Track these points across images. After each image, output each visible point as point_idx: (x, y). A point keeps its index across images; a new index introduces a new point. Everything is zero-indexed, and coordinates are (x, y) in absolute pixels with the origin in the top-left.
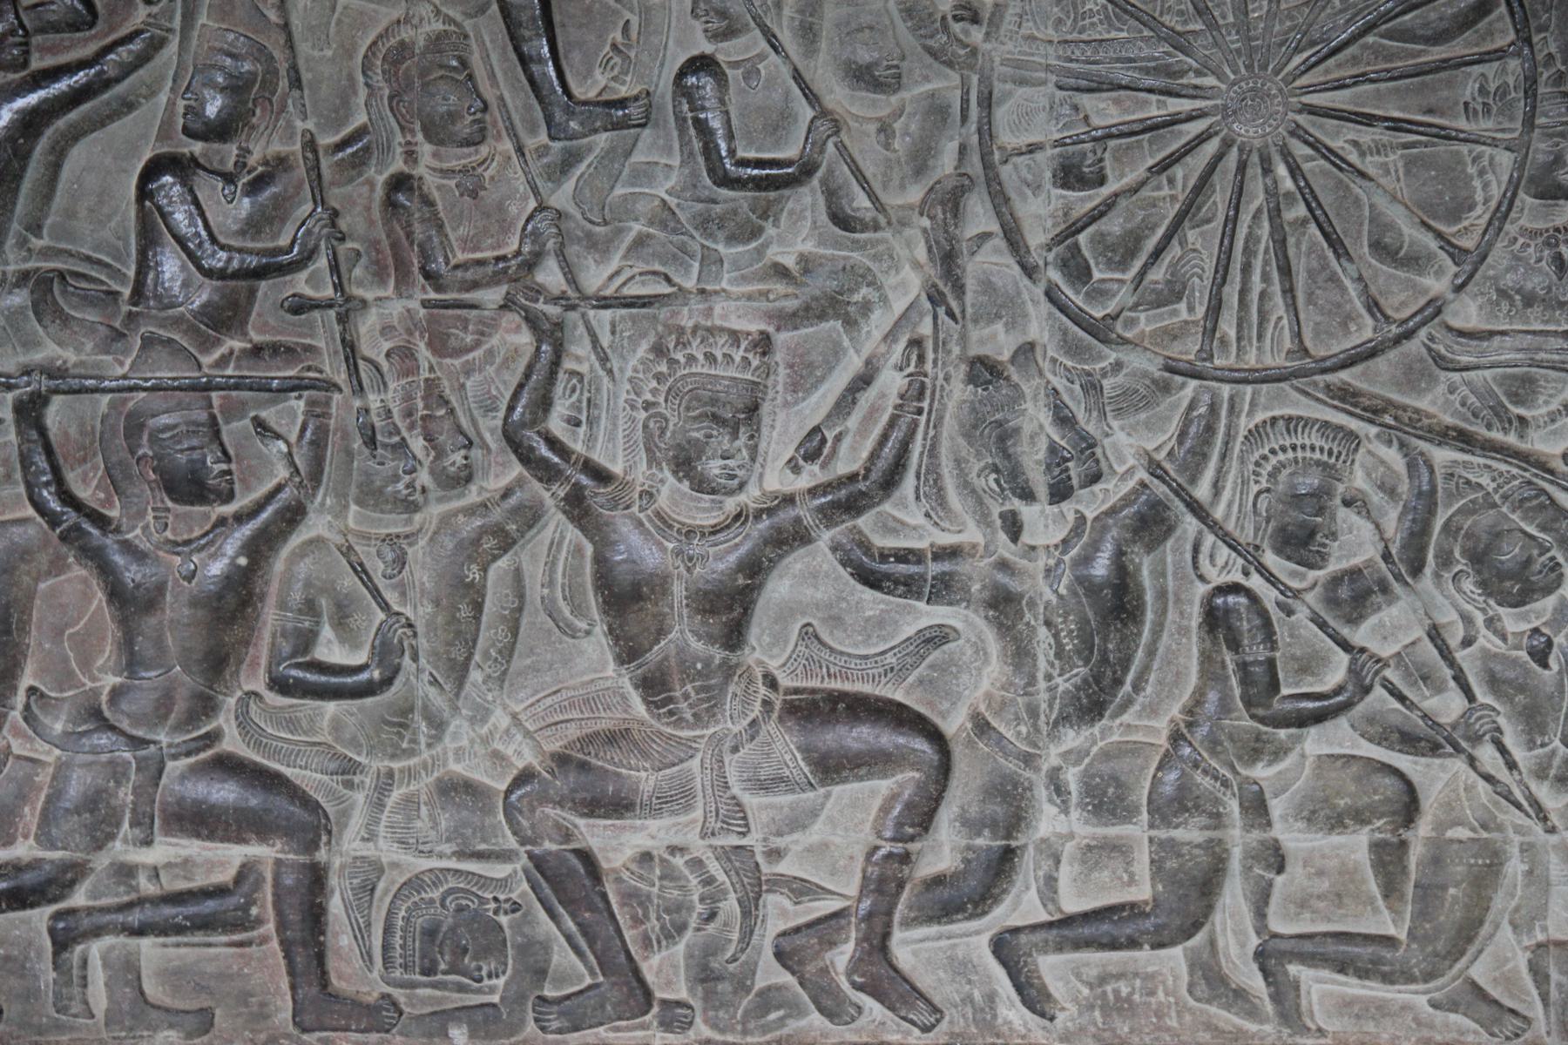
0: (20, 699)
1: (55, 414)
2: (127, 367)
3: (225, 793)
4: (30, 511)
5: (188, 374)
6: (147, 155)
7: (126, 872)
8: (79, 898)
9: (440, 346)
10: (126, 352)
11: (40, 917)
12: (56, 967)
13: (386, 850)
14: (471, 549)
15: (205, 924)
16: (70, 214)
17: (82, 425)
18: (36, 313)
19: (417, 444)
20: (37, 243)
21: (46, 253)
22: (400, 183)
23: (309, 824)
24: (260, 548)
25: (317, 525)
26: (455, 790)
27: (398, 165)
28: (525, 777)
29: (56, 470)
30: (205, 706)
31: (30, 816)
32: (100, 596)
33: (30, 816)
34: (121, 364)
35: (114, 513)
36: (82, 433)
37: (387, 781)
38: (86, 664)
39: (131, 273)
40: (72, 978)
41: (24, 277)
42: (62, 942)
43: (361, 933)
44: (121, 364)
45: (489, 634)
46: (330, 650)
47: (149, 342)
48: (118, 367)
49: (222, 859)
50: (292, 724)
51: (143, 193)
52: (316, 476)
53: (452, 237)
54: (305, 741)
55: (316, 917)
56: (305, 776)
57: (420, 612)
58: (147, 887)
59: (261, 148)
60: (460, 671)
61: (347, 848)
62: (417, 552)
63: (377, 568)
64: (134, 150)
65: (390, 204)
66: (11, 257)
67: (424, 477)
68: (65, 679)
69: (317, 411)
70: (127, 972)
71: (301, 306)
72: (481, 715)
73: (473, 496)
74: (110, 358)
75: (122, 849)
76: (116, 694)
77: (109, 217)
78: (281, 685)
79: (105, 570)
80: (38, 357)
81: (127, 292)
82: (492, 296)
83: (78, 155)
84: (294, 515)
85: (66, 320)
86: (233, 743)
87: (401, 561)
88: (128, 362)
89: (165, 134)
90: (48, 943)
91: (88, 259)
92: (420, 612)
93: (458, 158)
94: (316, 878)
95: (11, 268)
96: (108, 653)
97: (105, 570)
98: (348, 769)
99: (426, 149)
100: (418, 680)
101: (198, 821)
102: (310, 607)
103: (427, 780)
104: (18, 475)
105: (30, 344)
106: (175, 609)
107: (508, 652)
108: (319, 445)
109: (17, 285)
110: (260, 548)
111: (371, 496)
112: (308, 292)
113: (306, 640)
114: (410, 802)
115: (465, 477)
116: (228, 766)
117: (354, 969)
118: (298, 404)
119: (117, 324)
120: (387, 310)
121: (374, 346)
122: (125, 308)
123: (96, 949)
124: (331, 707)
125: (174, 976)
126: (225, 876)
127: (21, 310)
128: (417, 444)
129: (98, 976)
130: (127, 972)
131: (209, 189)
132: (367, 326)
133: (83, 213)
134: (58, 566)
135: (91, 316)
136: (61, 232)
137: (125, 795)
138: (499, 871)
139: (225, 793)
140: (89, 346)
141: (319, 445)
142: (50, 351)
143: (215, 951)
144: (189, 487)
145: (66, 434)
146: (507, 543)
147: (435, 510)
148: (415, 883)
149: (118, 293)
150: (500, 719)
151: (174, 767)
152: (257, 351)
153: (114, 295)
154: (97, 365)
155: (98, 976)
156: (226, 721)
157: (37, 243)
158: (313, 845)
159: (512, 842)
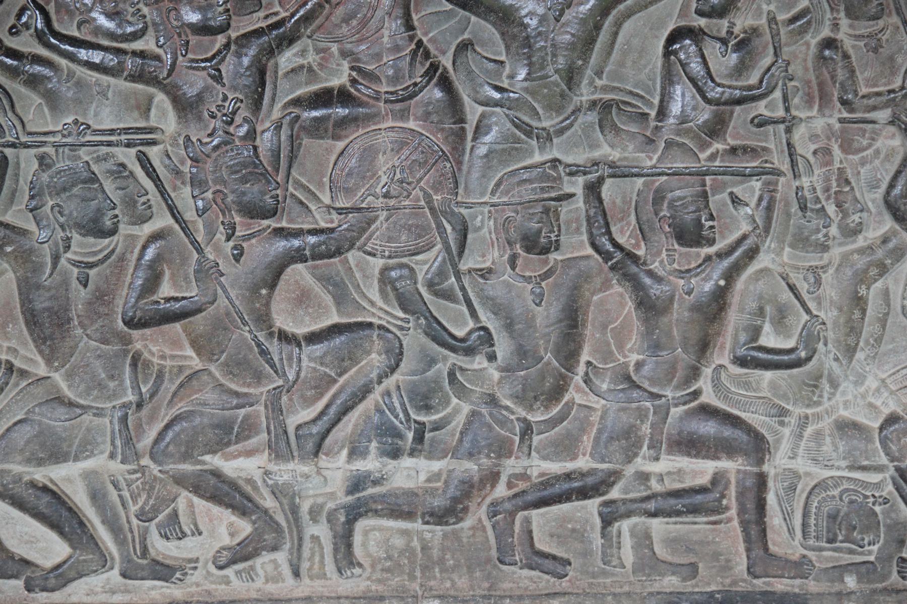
0: (581, 369)
1: (607, 191)
2: (654, 161)
3: (708, 428)
4: (590, 251)
5: (693, 165)
6: (671, 27)
7: (644, 477)
8: (615, 493)
9: (847, 148)
10: (654, 151)
11: (593, 505)
12: (603, 535)
13: (801, 465)
14: (863, 278)
15: (694, 510)
16: (621, 64)
17: (624, 197)
18: (601, 127)
19: (831, 209)
20: (599, 83)
21: (605, 89)
22: (829, 43)
23: (758, 446)
24: (730, 276)
25: (763, 260)
26: (847, 427)
27: (826, 32)
28: (892, 419)
29: (607, 225)
30: (694, 373)
31: (587, 442)
32: (630, 305)
33: (587, 442)
34: (651, 159)
35: (641, 252)
36: (624, 202)
37: (804, 421)
38: (621, 347)
39: (656, 101)
40: (610, 542)
41: (594, 103)
42: (607, 521)
43: (787, 517)
44: (651, 159)
45: (869, 329)
46: (769, 339)
47: (669, 144)
48: (649, 161)
49: (702, 470)
50: (747, 385)
51: (668, 53)
52: (767, 229)
53: (860, 78)
54: (755, 396)
55: (761, 506)
56: (755, 418)
57: (828, 315)
58: (655, 486)
59: (742, 22)
60: (851, 351)
61: (778, 463)
62: (827, 277)
63: (803, 288)
64: (662, 24)
65: (821, 58)
66: (584, 91)
67: (834, 230)
68: (607, 356)
69: (770, 189)
70: (644, 540)
71: (761, 123)
72: (860, 380)
73: (860, 242)
74: (643, 155)
75: (642, 464)
76: (639, 365)
77: (645, 67)
78: (742, 362)
79: (637, 287)
80: (596, 154)
81: (653, 113)
82: (883, 115)
83: (628, 26)
84: (752, 254)
85: (617, 130)
86: (709, 397)
87: (818, 282)
88: (656, 157)
89: (683, 14)
90: (598, 521)
91: (631, 93)
92: (828, 315)
93: (865, 27)
94: (762, 481)
95: (584, 99)
96: (634, 340)
97: (637, 287)
98: (783, 413)
99: (844, 22)
100: (826, 357)
101: (690, 445)
102: (761, 312)
103: (826, 424)
104: (584, 229)
105: (594, 146)
106: (679, 312)
107: (879, 340)
108: (769, 209)
109: (589, 109)
110: (730, 276)
111: (801, 241)
112: (767, 113)
113: (756, 332)
114: (818, 436)
115: (854, 232)
116: (708, 411)
117: (784, 539)
118: (756, 184)
119: (648, 134)
120: (815, 124)
121: (806, 149)
122: (653, 124)
123: (625, 526)
124: (768, 375)
125: (672, 542)
126: (704, 480)
127: (591, 125)
128: (831, 209)
129: (627, 542)
130: (644, 540)
131: (712, 49)
132: (800, 134)
133: (629, 64)
134: (606, 285)
135: (633, 128)
136: (616, 76)
137: (646, 429)
138: (874, 478)
139: (708, 428)
140: (631, 147)
141: (769, 209)
142: (606, 151)
143: (697, 527)
144: (690, 235)
145: (614, 203)
146: (883, 269)
147: (836, 252)
148: (821, 485)
149: (647, 114)
150: (872, 383)
151: (676, 412)
152: (733, 150)
153: (645, 115)
154: (635, 159)
155: (627, 542)
156: (704, 383)
157: (599, 83)
158: (760, 461)
159: (884, 460)
